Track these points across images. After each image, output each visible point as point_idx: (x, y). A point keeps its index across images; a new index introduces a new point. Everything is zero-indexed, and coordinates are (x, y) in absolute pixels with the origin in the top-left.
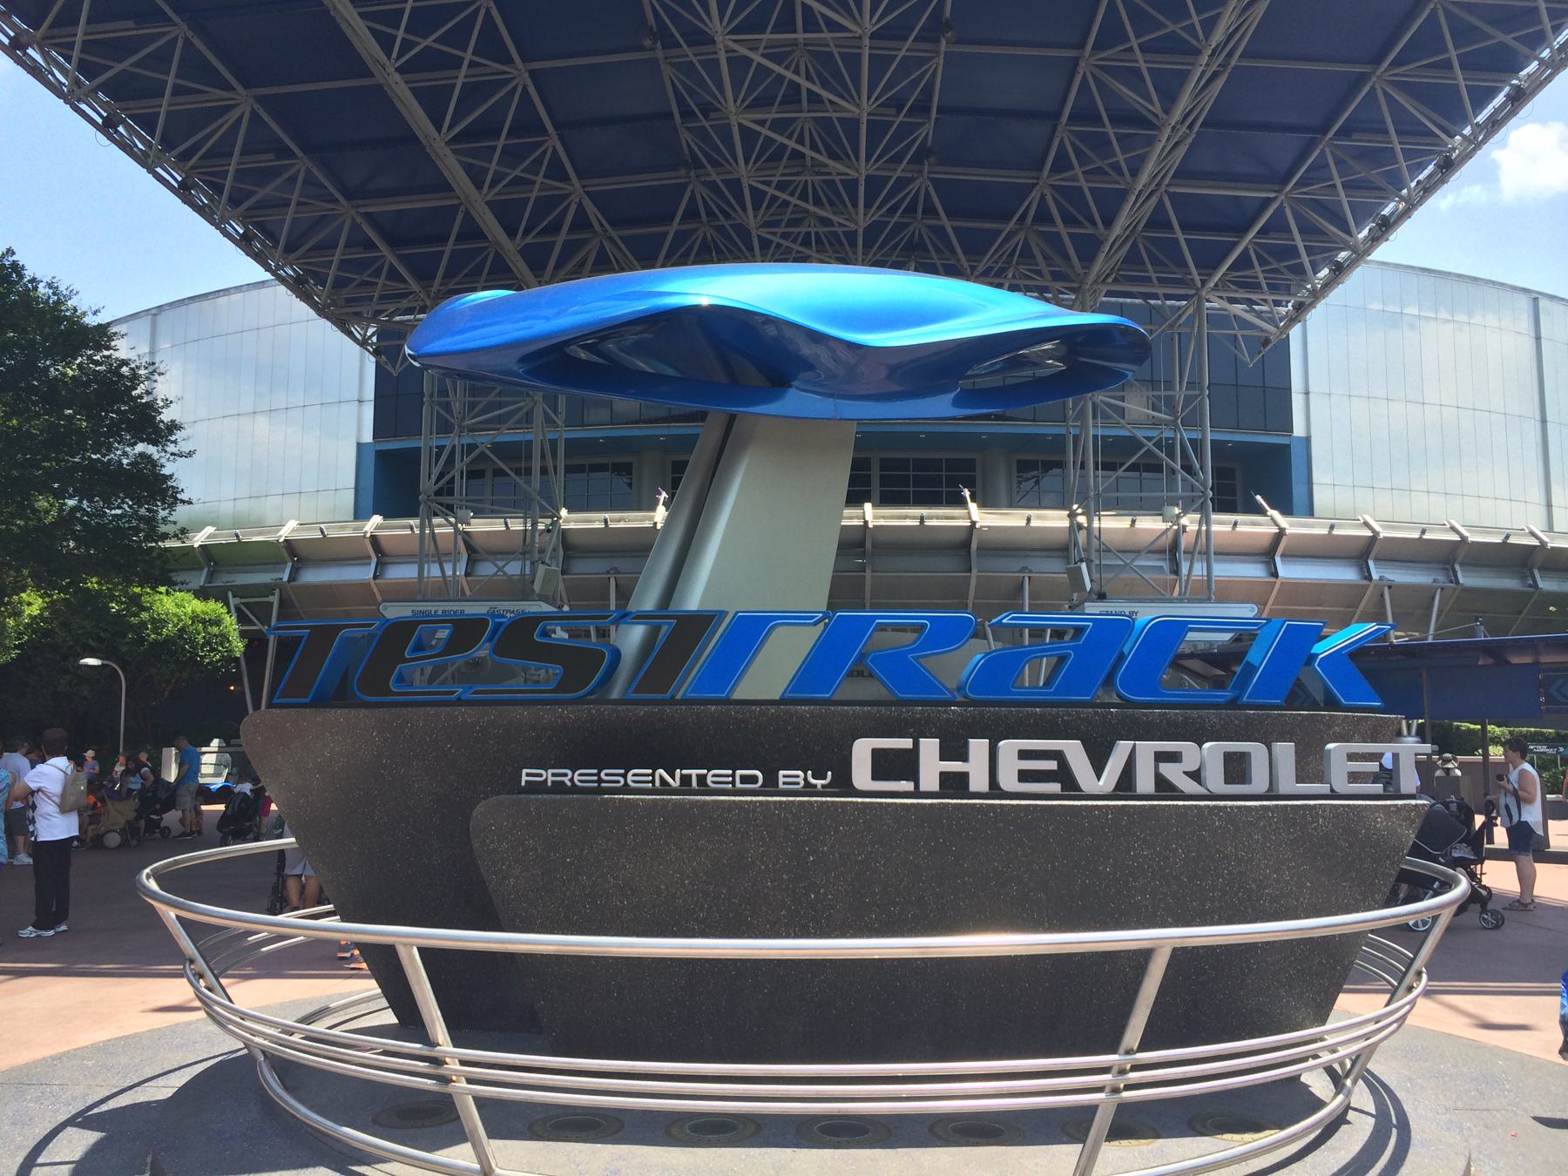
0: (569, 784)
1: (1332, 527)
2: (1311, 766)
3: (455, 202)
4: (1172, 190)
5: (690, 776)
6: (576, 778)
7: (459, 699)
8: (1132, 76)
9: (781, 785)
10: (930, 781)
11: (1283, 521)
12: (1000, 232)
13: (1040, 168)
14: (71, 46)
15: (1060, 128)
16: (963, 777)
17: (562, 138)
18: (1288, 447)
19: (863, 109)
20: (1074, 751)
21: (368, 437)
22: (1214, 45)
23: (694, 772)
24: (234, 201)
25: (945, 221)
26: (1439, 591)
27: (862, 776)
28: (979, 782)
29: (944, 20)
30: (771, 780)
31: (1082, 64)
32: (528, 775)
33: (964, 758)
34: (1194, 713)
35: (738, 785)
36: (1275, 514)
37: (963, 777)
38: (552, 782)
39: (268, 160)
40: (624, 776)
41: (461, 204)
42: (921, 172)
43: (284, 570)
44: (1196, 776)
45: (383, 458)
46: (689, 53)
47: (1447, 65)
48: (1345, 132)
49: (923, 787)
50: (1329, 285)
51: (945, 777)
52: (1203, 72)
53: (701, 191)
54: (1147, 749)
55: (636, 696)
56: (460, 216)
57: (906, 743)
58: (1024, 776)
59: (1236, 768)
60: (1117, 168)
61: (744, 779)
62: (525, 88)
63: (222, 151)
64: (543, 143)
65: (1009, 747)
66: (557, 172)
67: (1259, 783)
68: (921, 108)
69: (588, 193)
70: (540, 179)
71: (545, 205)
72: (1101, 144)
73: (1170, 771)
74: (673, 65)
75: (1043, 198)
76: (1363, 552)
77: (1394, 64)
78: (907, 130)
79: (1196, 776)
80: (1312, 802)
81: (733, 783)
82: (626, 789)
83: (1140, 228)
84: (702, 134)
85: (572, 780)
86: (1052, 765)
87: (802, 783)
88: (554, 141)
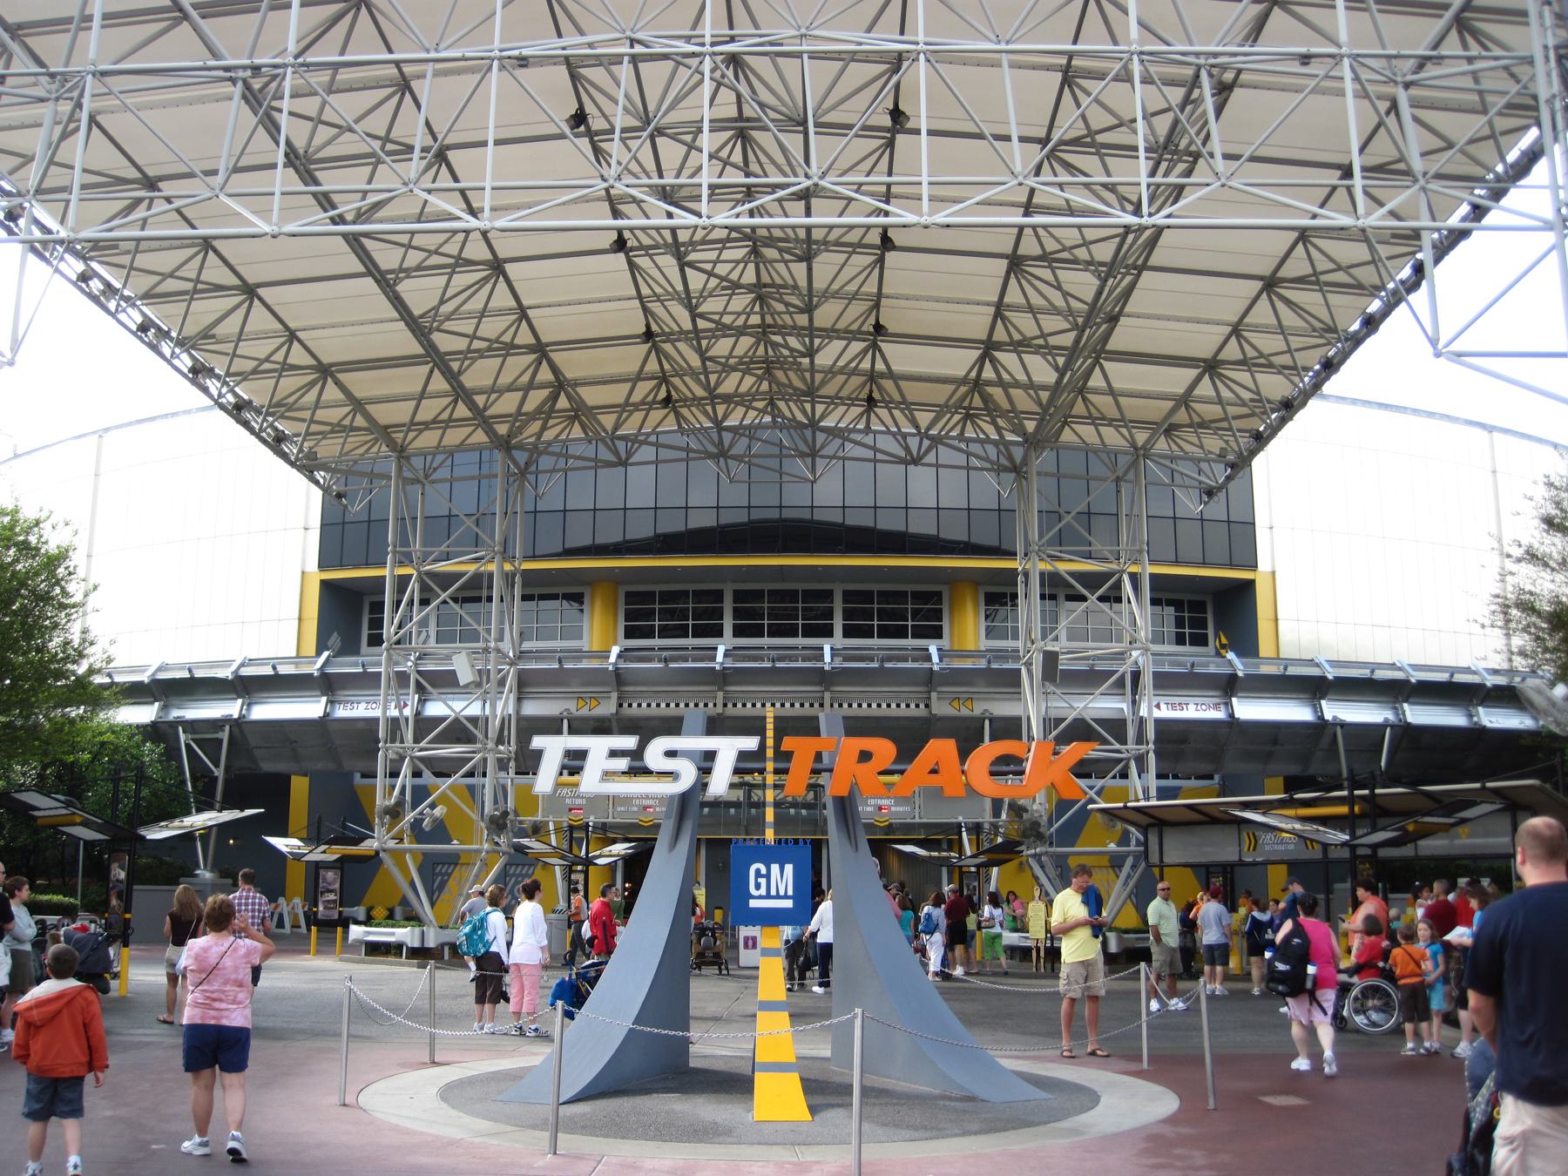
36: (1231, 655)
45: (325, 584)
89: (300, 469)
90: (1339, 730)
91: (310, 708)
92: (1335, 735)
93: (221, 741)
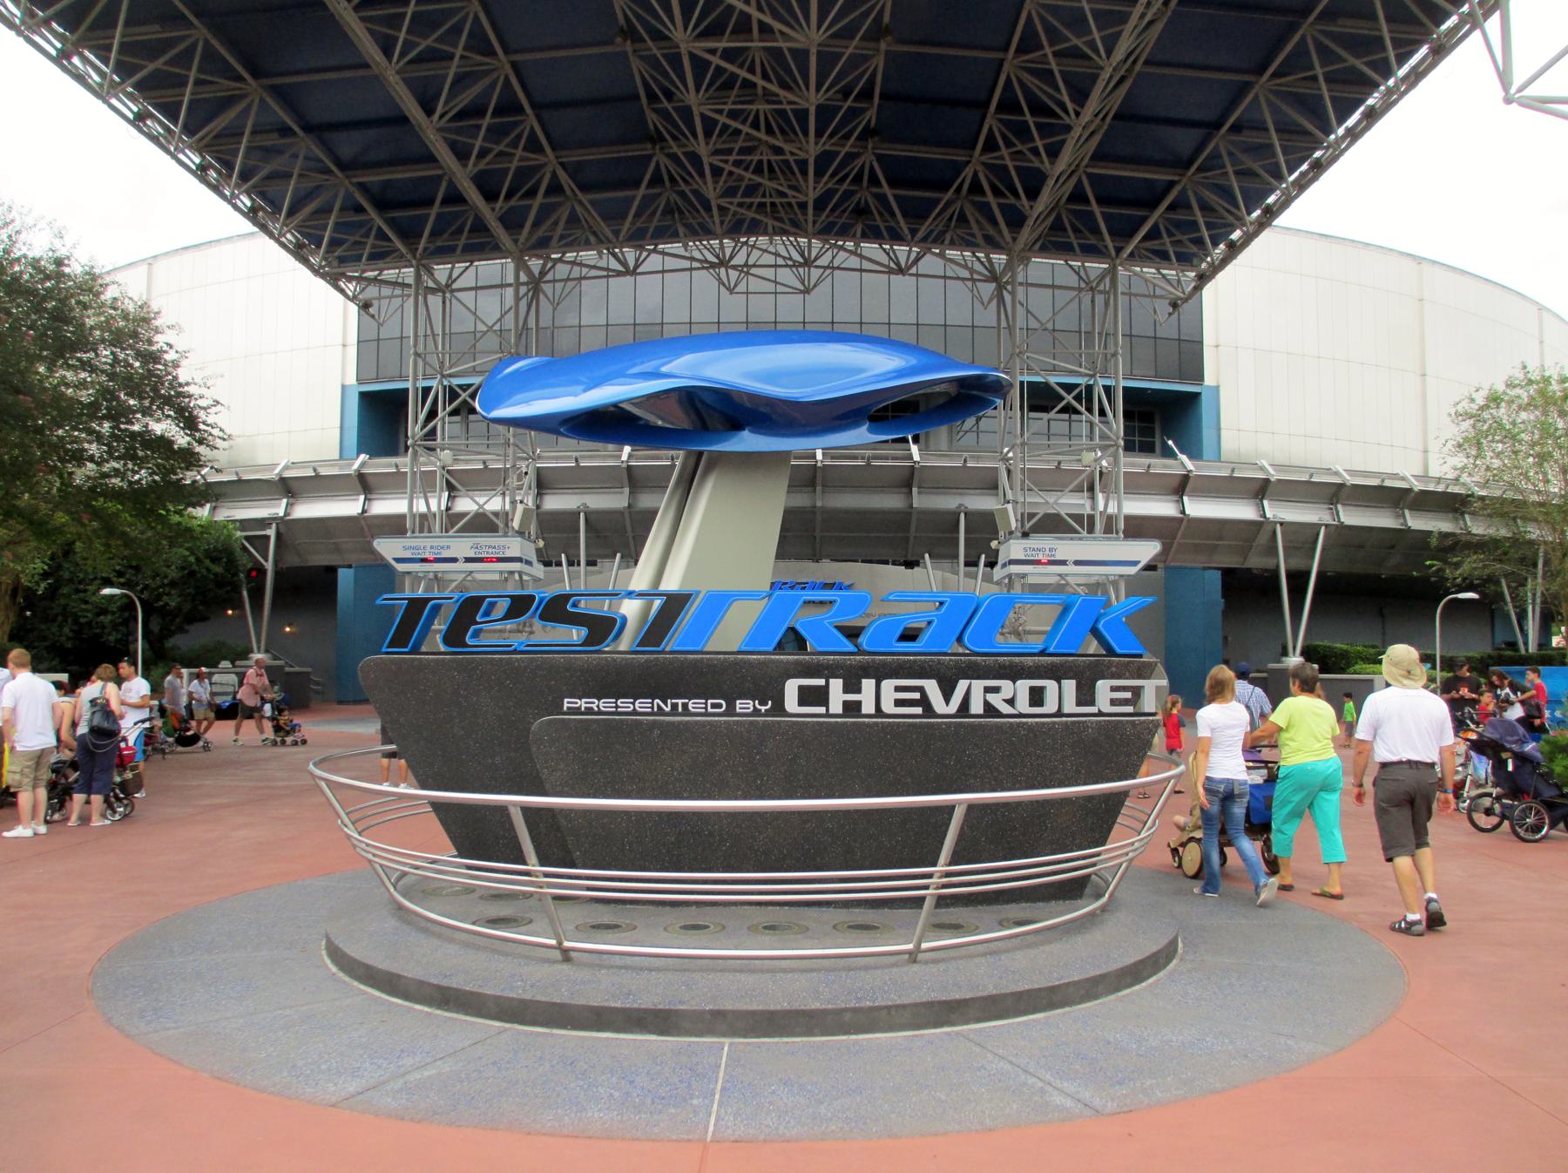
0: (596, 709)
1: (1233, 471)
3: (439, 172)
4: (1090, 170)
5: (677, 704)
6: (601, 705)
7: (515, 650)
8: (1047, 76)
9: (738, 710)
10: (836, 706)
11: (1190, 465)
12: (938, 201)
13: (973, 147)
14: (109, 48)
15: (989, 116)
16: (859, 703)
17: (538, 117)
18: (1197, 395)
19: (812, 99)
20: (932, 687)
21: (352, 379)
22: (1114, 64)
23: (680, 702)
24: (245, 176)
25: (886, 189)
26: (1323, 528)
27: (791, 703)
28: (868, 707)
29: (884, 25)
31: (1006, 67)
32: (568, 703)
33: (859, 691)
34: (1017, 659)
35: (710, 710)
36: (1183, 457)
37: (859, 703)
38: (586, 708)
39: (273, 140)
40: (633, 703)
41: (445, 174)
42: (866, 148)
43: (280, 506)
44: (1011, 702)
46: (654, 49)
47: (1314, 79)
48: (1236, 129)
49: (831, 712)
50: (1225, 261)
51: (846, 704)
52: (1111, 77)
53: (664, 161)
54: (978, 686)
55: (638, 649)
56: (444, 185)
57: (821, 682)
58: (899, 703)
59: (1037, 697)
60: (1035, 152)
61: (714, 706)
62: (507, 79)
63: (233, 133)
64: (522, 122)
65: (888, 685)
66: (533, 146)
67: (1050, 706)
68: (866, 95)
69: (562, 165)
70: (519, 152)
71: (523, 174)
72: (1022, 132)
73: (995, 700)
74: (641, 57)
75: (975, 174)
76: (1261, 490)
77: (1275, 75)
78: (853, 113)
79: (1011, 702)
80: (1084, 719)
81: (706, 708)
82: (635, 712)
83: (1064, 199)
84: (664, 114)
85: (598, 706)
86: (917, 696)
87: (752, 709)
88: (531, 121)
89: (323, 276)
90: (1278, 528)
91: (349, 507)
92: (1274, 532)
93: (268, 537)
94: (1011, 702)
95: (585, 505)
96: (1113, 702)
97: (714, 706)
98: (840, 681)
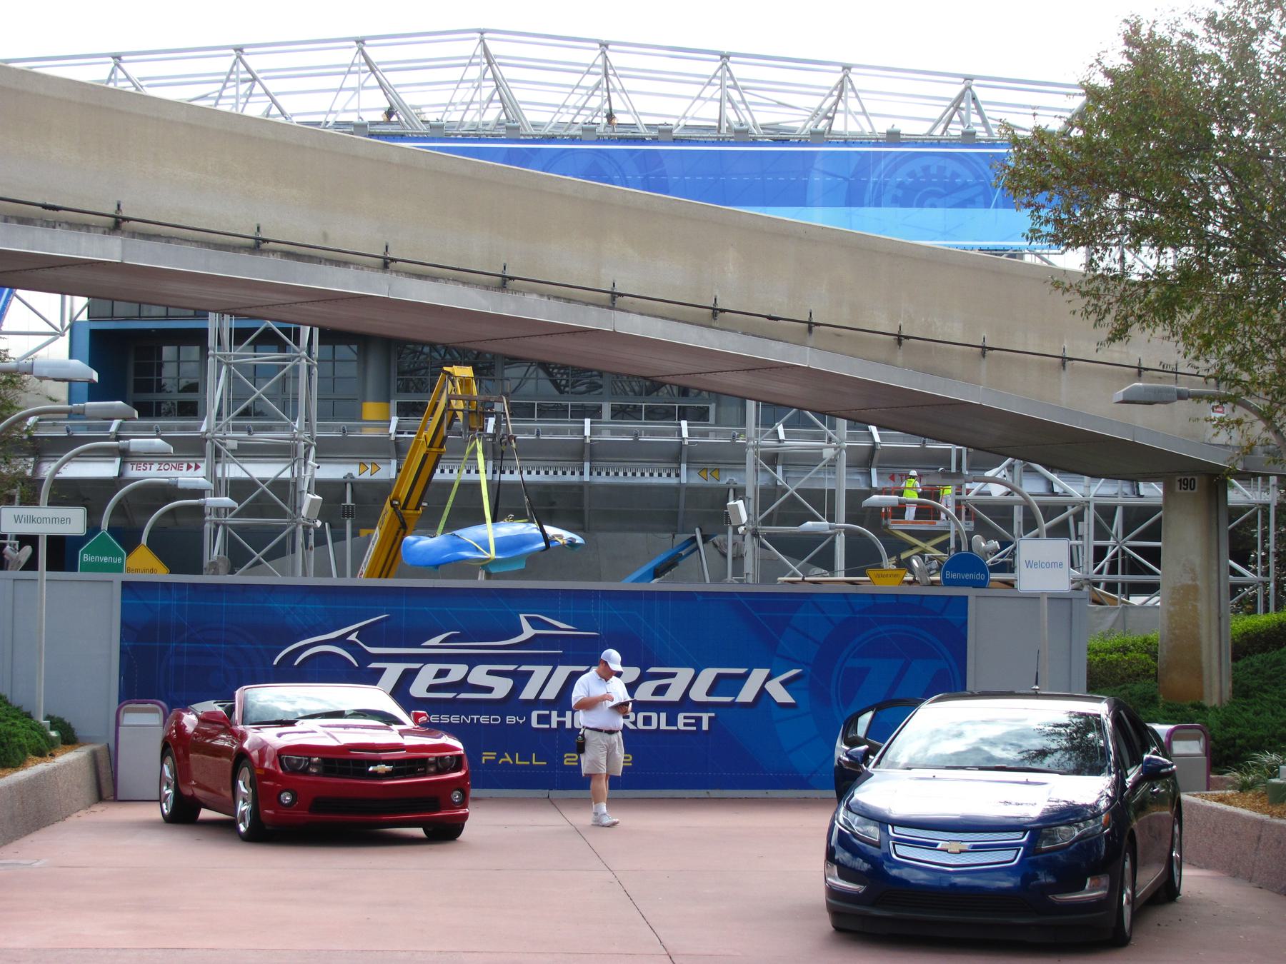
2: (672, 721)
10: (554, 725)
23: (475, 717)
28: (568, 725)
30: (503, 720)
33: (565, 717)
40: (449, 718)
57: (547, 712)
59: (647, 721)
61: (494, 720)
94: (635, 723)
95: (350, 474)
96: (685, 724)
97: (494, 720)
98: (556, 712)
